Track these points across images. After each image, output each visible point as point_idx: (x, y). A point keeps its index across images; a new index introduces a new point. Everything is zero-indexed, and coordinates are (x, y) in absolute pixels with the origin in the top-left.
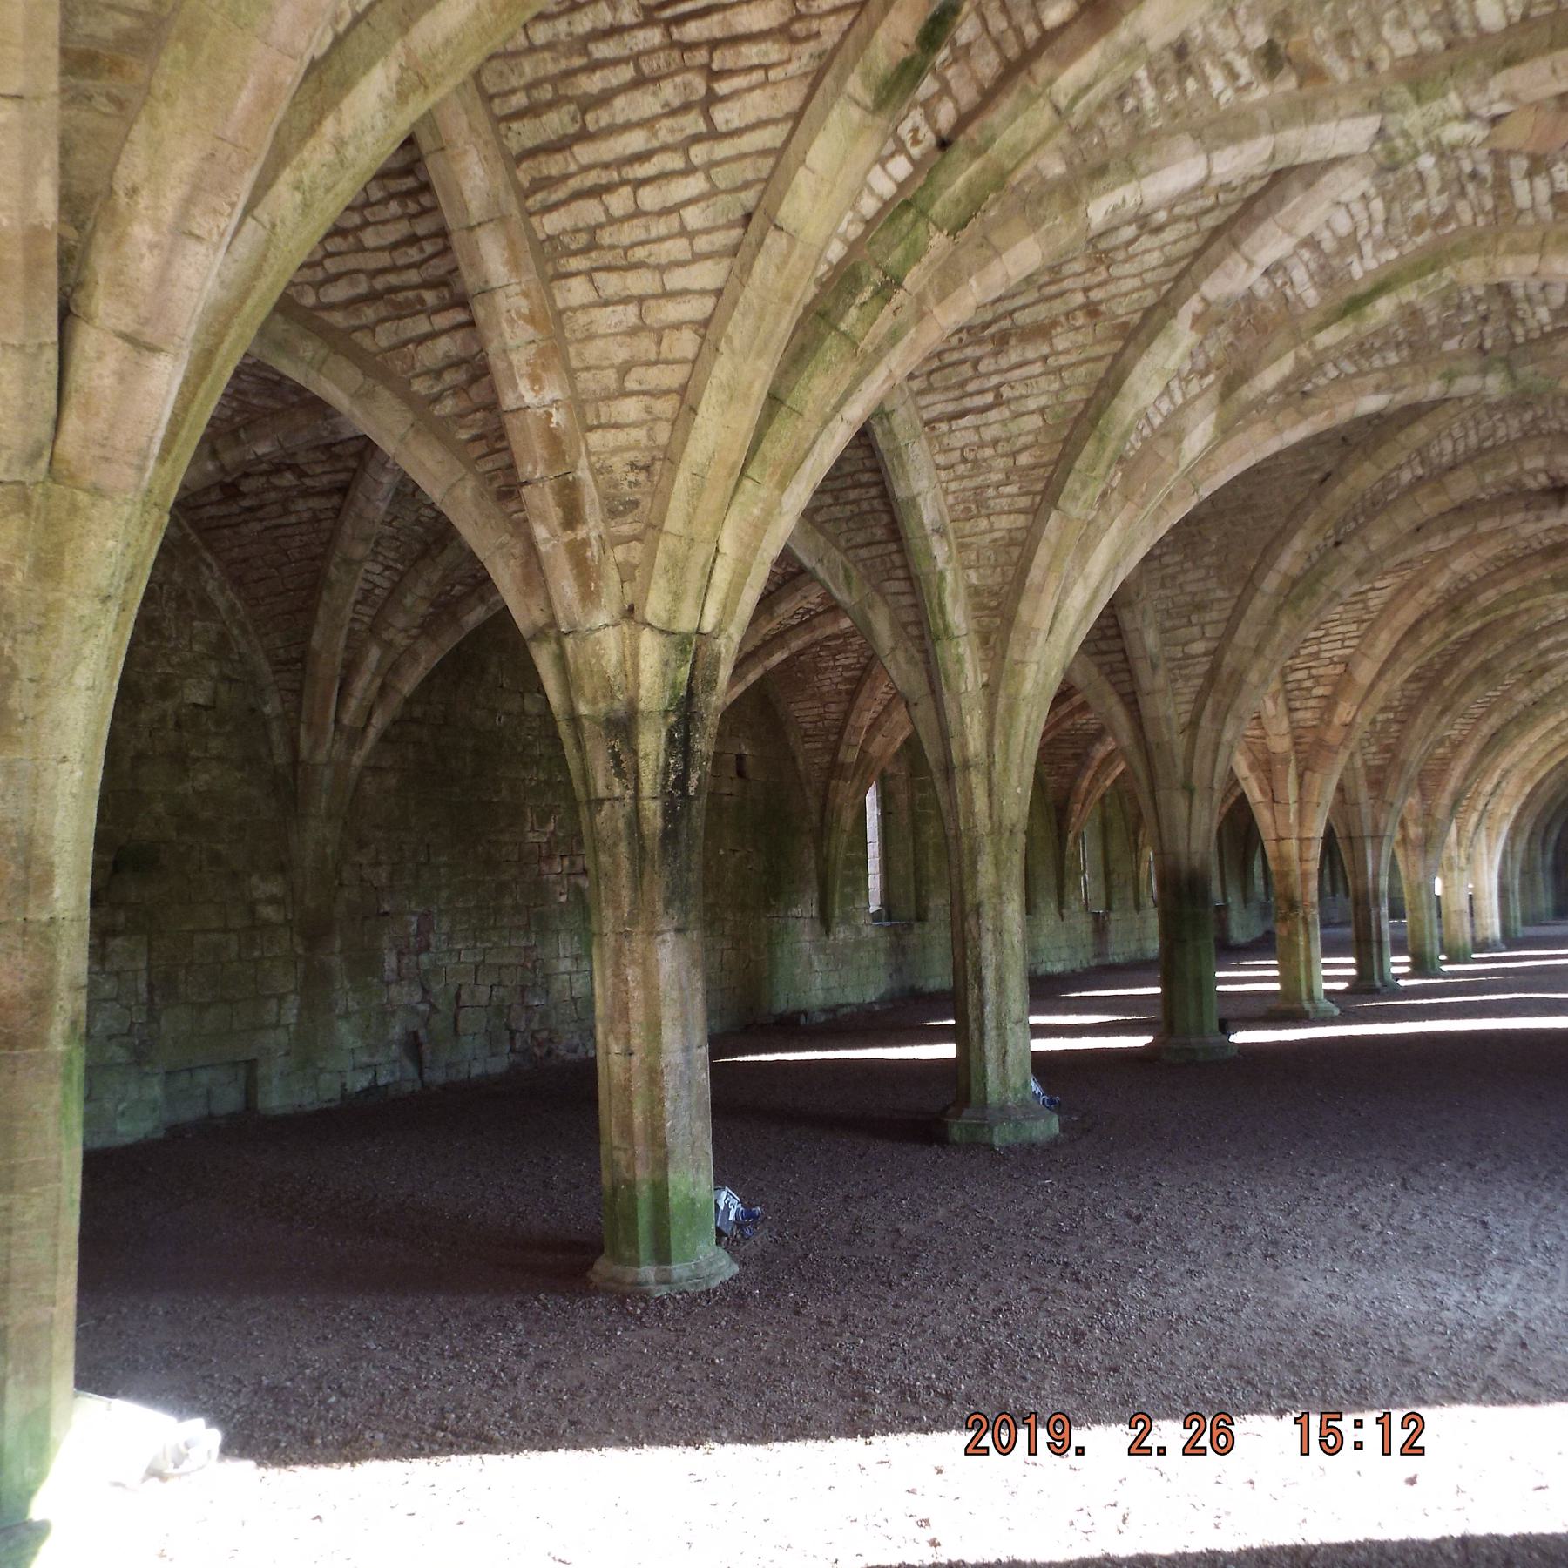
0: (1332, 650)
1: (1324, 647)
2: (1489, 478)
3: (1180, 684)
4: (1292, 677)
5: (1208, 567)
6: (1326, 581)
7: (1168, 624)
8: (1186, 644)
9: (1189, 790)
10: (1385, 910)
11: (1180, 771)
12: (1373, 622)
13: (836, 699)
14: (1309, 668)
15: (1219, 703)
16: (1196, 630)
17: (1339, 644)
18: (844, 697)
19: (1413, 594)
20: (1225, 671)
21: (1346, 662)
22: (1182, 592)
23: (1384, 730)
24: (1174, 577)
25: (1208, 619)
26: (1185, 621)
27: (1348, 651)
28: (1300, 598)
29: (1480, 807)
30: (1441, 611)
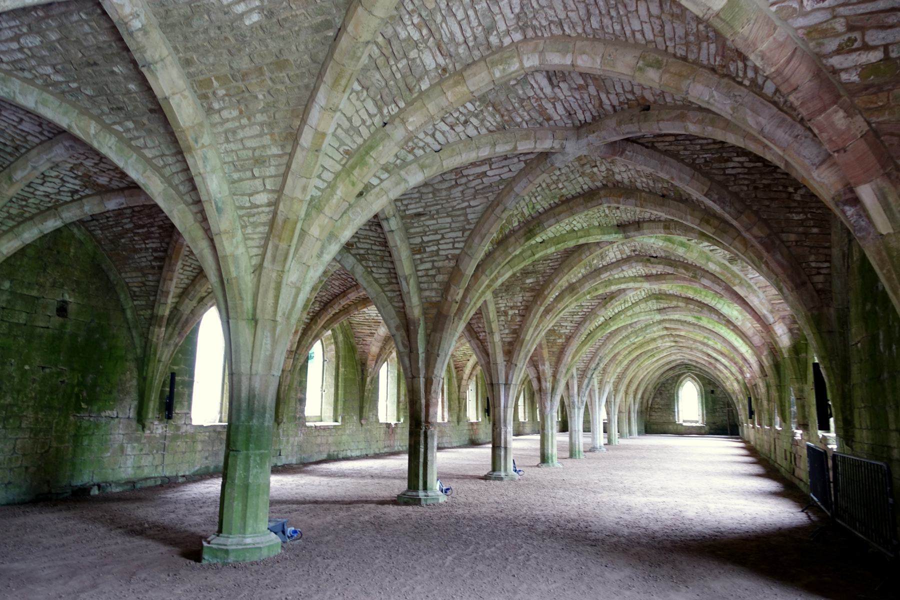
0: (446, 249)
1: (441, 247)
2: (498, 74)
3: (249, 230)
4: (421, 267)
5: (262, 125)
7: (236, 176)
8: (251, 195)
9: (254, 320)
10: (510, 429)
11: (248, 304)
12: (472, 231)
13: (151, 271)
14: (433, 261)
15: (276, 247)
16: (258, 183)
18: (156, 271)
19: (493, 211)
20: (280, 219)
21: (457, 259)
22: (244, 148)
23: (512, 320)
24: (234, 132)
25: (268, 174)
26: (249, 174)
27: (457, 252)
28: (353, 167)
29: (589, 376)
30: (521, 232)
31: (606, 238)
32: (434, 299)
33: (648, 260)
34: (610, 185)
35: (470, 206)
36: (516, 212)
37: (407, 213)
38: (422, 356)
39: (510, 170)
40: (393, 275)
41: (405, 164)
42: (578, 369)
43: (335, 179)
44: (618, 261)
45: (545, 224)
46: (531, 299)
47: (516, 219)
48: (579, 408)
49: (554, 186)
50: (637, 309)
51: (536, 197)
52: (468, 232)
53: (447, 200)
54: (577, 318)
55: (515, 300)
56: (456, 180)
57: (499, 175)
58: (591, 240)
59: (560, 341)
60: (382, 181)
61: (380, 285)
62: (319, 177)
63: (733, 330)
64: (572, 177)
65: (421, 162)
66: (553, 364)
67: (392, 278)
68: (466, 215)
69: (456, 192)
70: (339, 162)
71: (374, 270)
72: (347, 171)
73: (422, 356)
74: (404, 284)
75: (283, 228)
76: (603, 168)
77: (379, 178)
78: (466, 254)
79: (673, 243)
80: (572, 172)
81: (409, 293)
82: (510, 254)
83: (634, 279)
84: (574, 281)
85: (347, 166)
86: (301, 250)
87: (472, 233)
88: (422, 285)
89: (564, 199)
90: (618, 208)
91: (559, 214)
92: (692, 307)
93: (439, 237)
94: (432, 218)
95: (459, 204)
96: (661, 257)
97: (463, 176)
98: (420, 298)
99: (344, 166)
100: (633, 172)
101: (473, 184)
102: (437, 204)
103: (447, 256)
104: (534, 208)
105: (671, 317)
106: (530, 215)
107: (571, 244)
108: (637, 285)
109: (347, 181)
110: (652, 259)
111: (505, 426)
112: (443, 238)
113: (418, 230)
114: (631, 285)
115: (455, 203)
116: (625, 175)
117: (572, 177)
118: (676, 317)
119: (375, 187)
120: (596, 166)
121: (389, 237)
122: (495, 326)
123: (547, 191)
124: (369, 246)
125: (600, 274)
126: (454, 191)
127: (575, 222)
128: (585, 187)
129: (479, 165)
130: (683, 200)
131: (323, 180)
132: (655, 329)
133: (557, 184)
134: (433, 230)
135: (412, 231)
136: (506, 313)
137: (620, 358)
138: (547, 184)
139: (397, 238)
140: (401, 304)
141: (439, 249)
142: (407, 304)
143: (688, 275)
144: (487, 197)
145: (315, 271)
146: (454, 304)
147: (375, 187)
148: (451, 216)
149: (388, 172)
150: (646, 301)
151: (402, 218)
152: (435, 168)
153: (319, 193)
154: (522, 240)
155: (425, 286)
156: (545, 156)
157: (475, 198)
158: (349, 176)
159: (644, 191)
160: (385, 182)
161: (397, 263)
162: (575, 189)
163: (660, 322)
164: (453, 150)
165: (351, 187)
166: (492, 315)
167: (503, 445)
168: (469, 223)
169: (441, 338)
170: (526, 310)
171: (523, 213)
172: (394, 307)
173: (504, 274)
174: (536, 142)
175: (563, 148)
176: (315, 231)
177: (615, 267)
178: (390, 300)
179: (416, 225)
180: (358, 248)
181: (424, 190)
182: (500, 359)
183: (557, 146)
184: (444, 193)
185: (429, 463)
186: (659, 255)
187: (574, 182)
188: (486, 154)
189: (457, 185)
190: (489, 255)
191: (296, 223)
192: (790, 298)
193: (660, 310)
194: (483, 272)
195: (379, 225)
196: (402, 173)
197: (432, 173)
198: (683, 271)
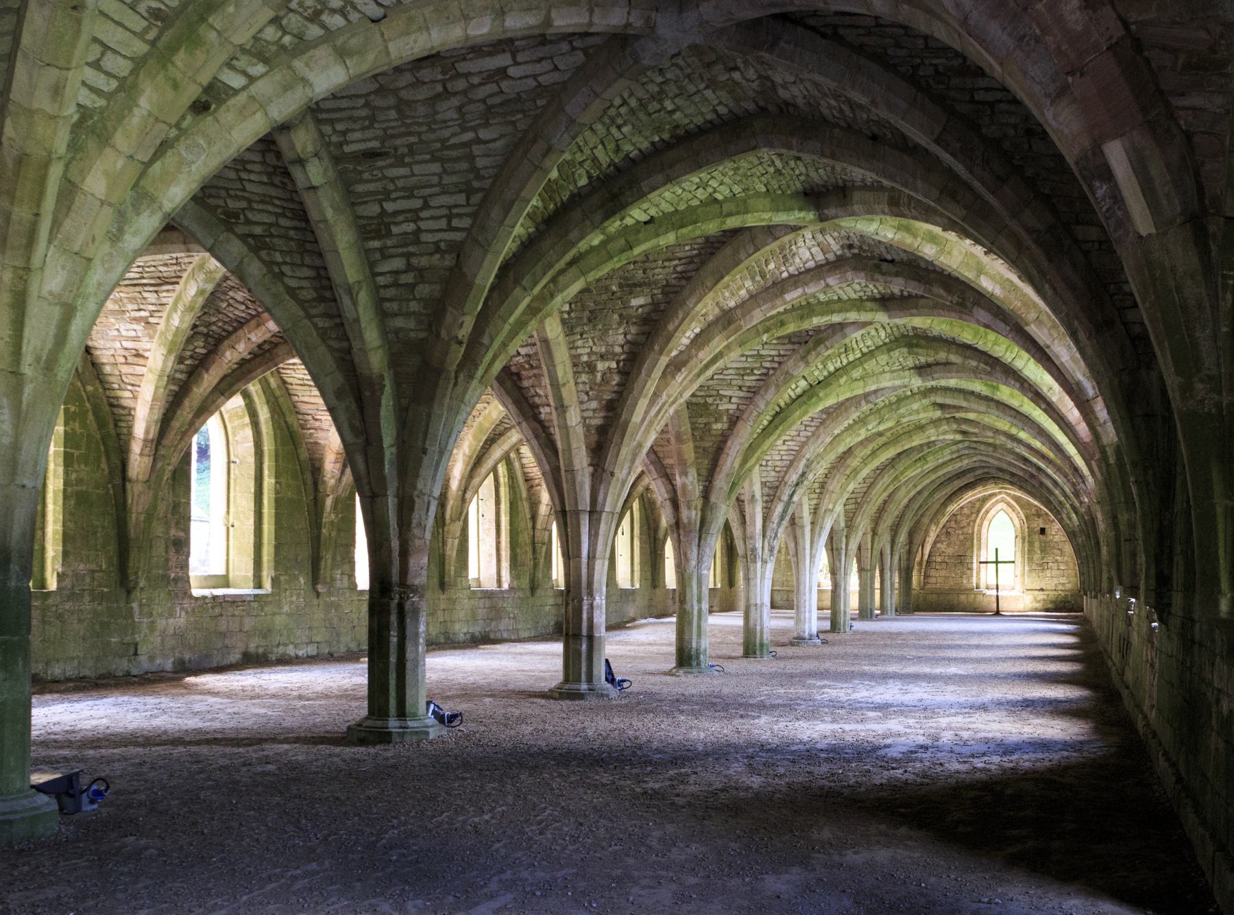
0: (433, 229)
1: (423, 225)
4: (385, 267)
6: (215, 20)
14: (408, 256)
17: (443, 223)
21: (457, 250)
27: (458, 236)
28: (173, 49)
29: (785, 498)
31: (781, 218)
32: (412, 335)
33: (877, 268)
34: (771, 108)
35: (478, 141)
36: (579, 157)
37: (347, 149)
38: (389, 453)
39: (556, 68)
40: (325, 282)
41: (302, 46)
42: (764, 484)
43: (135, 72)
44: (819, 267)
45: (644, 185)
46: (642, 339)
47: (582, 171)
48: (764, 562)
49: (654, 106)
50: (870, 365)
51: (619, 127)
52: (480, 196)
53: (429, 124)
54: (750, 380)
55: (610, 340)
56: (444, 82)
57: (535, 77)
58: (751, 220)
59: (718, 426)
60: (252, 79)
61: (301, 303)
62: (96, 65)
63: (1044, 410)
64: (691, 88)
65: (339, 42)
66: (704, 472)
67: (324, 288)
68: (471, 158)
69: (447, 109)
70: (140, 35)
71: (286, 269)
72: (159, 56)
73: (389, 453)
74: (346, 301)
75: (17, 174)
76: (751, 74)
77: (245, 73)
78: (476, 241)
79: (915, 236)
80: (688, 76)
81: (357, 320)
82: (573, 244)
83: (858, 304)
84: (732, 304)
85: (160, 45)
86: (67, 225)
87: (487, 196)
88: (387, 305)
89: (681, 132)
90: (799, 159)
91: (671, 166)
92: (974, 363)
93: (418, 203)
94: (400, 162)
95: (454, 135)
96: (902, 262)
97: (459, 75)
98: (384, 332)
99: (153, 43)
100: (808, 85)
101: (481, 93)
102: (409, 134)
103: (436, 243)
104: (618, 149)
105: (943, 383)
106: (612, 163)
107: (712, 228)
108: (864, 317)
109: (160, 77)
110: (885, 266)
111: (591, 594)
112: (426, 206)
113: (371, 187)
114: (852, 316)
115: (446, 133)
116: (795, 90)
117: (691, 88)
118: (952, 383)
119: (236, 92)
120: (736, 68)
121: (308, 200)
122: (570, 394)
123: (641, 115)
124: (271, 219)
125: (783, 292)
126: (442, 106)
127: (714, 183)
128: (722, 110)
129: (490, 54)
130: (906, 146)
131: (108, 74)
132: (915, 406)
133: (660, 101)
134: (404, 189)
135: (360, 188)
136: (591, 368)
137: (854, 462)
138: (640, 100)
139: (326, 204)
140: (345, 344)
141: (419, 230)
142: (356, 345)
143: (949, 299)
144: (513, 123)
145: (108, 271)
146: (454, 346)
147: (236, 92)
148: (442, 160)
149: (266, 61)
150: (889, 350)
151: (336, 160)
152: (371, 57)
153: (101, 103)
154: (598, 217)
155: (395, 306)
156: (621, 40)
157: (486, 124)
158: (164, 67)
159: (837, 125)
160: (259, 83)
161: (329, 257)
162: (702, 114)
163: (926, 392)
164: (411, 20)
165: (170, 94)
166: (564, 370)
167: (584, 632)
168: (479, 177)
169: (429, 415)
170: (632, 364)
171: (595, 159)
172: (330, 347)
173: (567, 286)
174: (591, 12)
175: (651, 27)
176: (95, 184)
177: (812, 280)
178: (323, 335)
179: (366, 176)
180: (249, 222)
181: (378, 102)
182: (581, 460)
183: (637, 21)
184: (422, 110)
185: (409, 665)
186: (897, 258)
187: (697, 98)
188: (485, 30)
189: (447, 94)
190: (528, 245)
191: (46, 165)
192: (1089, 351)
193: (921, 370)
194: (517, 281)
195: (287, 174)
196: (298, 64)
197: (365, 67)
198: (942, 292)
